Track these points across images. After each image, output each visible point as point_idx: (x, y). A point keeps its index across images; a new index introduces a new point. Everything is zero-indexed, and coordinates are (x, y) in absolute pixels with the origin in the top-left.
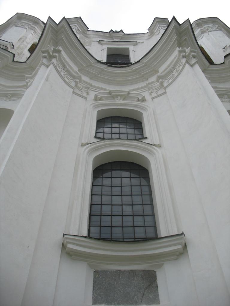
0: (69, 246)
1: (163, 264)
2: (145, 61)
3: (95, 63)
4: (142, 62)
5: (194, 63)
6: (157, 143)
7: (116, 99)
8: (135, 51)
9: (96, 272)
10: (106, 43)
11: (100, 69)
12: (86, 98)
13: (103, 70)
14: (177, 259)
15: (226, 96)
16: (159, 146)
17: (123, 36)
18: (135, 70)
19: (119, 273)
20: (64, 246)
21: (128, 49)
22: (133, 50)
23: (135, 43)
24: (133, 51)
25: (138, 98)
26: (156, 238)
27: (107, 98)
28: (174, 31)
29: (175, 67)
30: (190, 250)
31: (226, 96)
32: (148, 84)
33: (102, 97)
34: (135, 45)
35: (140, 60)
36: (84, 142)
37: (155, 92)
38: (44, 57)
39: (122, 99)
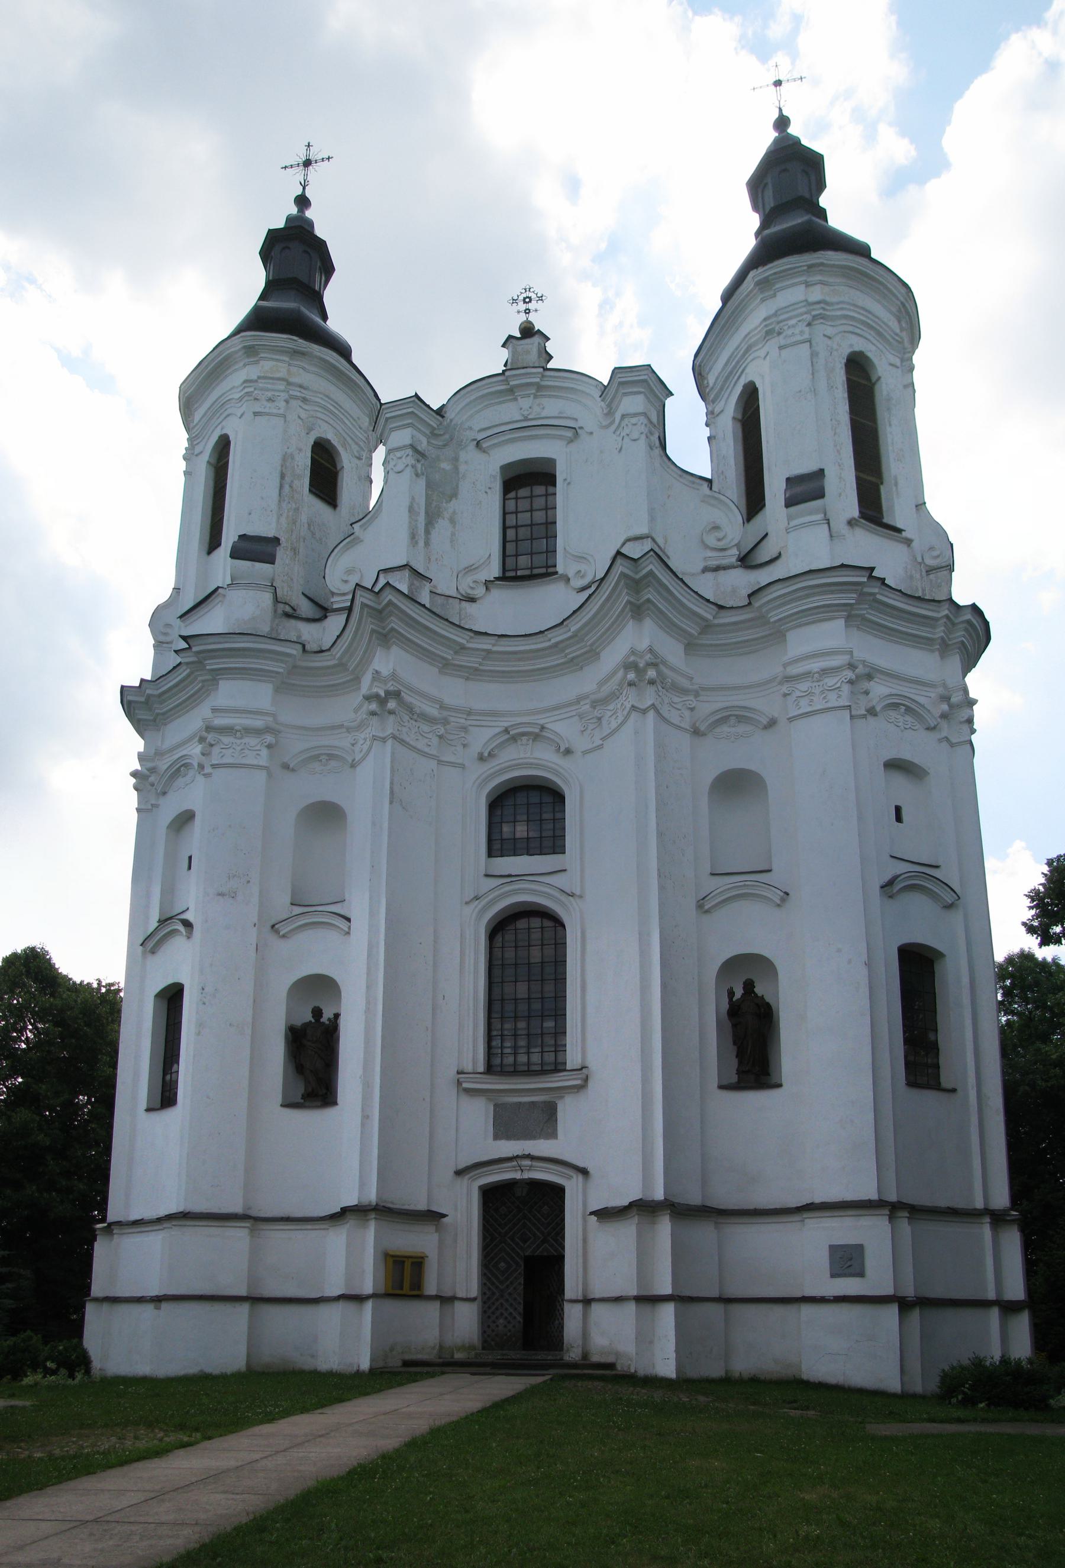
0: (465, 1085)
1: (563, 1097)
2: (574, 626)
3: (471, 638)
4: (567, 626)
5: (648, 708)
6: (578, 893)
7: (519, 740)
8: (569, 484)
9: (496, 1106)
10: (496, 441)
11: (483, 650)
12: (463, 766)
13: (489, 652)
14: (578, 1092)
15: (733, 720)
16: (581, 897)
17: (543, 376)
18: (556, 645)
19: (520, 1104)
20: (459, 1083)
22: (565, 480)
23: (569, 434)
24: (568, 481)
25: (558, 744)
26: (558, 1067)
27: (501, 746)
28: (622, 583)
29: (621, 688)
30: (590, 1084)
31: (733, 720)
32: (579, 700)
33: (492, 750)
34: (571, 441)
35: (564, 620)
36: (467, 900)
37: (589, 731)
38: (373, 713)
39: (531, 741)
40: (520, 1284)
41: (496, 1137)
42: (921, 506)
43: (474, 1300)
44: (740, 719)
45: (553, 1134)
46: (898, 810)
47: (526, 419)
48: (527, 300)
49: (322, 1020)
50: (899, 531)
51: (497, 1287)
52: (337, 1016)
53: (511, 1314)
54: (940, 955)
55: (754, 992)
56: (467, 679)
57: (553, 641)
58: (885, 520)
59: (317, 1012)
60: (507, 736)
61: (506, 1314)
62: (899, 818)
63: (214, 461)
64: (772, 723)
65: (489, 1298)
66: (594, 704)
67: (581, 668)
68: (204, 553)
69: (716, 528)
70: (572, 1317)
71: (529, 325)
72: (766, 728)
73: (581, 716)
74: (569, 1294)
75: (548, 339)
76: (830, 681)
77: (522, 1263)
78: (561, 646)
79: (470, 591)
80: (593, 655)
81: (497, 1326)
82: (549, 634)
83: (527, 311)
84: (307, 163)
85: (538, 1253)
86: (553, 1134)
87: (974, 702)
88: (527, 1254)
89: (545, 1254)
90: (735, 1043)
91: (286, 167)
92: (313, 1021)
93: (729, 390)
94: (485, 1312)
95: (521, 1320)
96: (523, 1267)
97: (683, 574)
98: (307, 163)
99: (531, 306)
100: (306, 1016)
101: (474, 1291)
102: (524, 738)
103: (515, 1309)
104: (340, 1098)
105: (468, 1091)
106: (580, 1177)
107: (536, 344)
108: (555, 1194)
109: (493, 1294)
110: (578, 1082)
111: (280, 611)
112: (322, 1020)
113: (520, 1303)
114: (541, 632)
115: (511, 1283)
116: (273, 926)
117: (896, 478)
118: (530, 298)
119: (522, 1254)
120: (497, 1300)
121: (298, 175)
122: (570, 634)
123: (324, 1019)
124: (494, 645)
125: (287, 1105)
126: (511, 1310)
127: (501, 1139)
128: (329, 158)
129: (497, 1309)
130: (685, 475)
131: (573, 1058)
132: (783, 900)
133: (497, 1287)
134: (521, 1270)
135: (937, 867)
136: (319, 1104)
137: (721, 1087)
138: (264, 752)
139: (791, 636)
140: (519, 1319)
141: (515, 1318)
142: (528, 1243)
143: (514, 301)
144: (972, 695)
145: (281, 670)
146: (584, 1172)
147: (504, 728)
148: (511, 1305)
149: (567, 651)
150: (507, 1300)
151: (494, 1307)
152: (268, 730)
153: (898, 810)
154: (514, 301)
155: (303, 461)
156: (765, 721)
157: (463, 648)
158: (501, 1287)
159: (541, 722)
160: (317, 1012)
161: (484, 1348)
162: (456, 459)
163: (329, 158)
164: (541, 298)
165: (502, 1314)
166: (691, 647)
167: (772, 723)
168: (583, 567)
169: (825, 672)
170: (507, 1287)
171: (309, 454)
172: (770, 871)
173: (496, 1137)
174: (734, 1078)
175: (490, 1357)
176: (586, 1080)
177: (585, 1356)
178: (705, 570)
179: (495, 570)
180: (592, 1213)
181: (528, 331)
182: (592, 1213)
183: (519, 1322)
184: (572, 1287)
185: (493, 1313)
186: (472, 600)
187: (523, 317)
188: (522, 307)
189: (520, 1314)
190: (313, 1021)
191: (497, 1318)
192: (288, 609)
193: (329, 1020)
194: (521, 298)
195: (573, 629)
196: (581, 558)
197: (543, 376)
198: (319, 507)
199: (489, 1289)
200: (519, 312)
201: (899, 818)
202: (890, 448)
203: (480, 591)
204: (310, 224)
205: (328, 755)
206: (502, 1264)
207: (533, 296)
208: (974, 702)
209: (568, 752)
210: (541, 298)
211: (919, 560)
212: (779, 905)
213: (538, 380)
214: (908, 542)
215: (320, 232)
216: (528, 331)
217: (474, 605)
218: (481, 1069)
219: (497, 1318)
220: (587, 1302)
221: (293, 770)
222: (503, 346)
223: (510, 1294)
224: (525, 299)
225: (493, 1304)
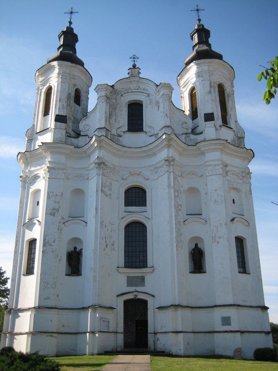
0: (120, 271)
2: (150, 147)
6: (150, 217)
8: (146, 108)
13: (126, 151)
18: (144, 151)
21: (142, 101)
30: (155, 271)
32: (150, 166)
41: (128, 286)
42: (236, 121)
43: (122, 333)
44: (193, 174)
45: (144, 286)
46: (233, 200)
47: (135, 89)
48: (134, 58)
49: (76, 250)
50: (232, 129)
52: (81, 249)
54: (245, 239)
55: (198, 247)
56: (120, 158)
57: (144, 150)
58: (228, 126)
59: (75, 248)
60: (130, 174)
62: (234, 203)
63: (46, 91)
64: (202, 176)
66: (156, 168)
67: (151, 157)
68: (43, 116)
69: (186, 123)
70: (151, 338)
71: (135, 65)
72: (200, 177)
73: (151, 170)
74: (149, 331)
75: (140, 69)
76: (217, 167)
78: (146, 151)
79: (120, 134)
80: (155, 154)
82: (143, 148)
83: (134, 61)
84: (71, 13)
85: (139, 319)
86: (144, 286)
87: (251, 173)
88: (137, 319)
89: (142, 320)
90: (193, 261)
91: (65, 13)
92: (74, 250)
93: (187, 87)
94: (124, 337)
97: (178, 135)
98: (71, 13)
99: (135, 60)
100: (73, 249)
101: (122, 331)
102: (135, 175)
104: (83, 273)
105: (120, 273)
106: (152, 297)
107: (137, 70)
108: (145, 302)
109: (127, 331)
110: (151, 271)
111: (67, 135)
112: (76, 250)
113: (134, 334)
114: (141, 147)
116: (64, 223)
117: (230, 115)
118: (135, 58)
119: (135, 320)
121: (69, 16)
122: (148, 149)
123: (77, 250)
124: (127, 150)
125: (67, 275)
127: (129, 286)
128: (78, 12)
129: (128, 336)
130: (177, 109)
131: (149, 263)
132: (205, 223)
134: (135, 324)
135: (244, 215)
136: (76, 275)
137: (190, 273)
138: (63, 175)
139: (206, 154)
140: (135, 339)
142: (137, 317)
143: (131, 58)
144: (250, 171)
145: (68, 153)
146: (153, 296)
147: (129, 172)
148: (132, 335)
149: (147, 153)
151: (127, 335)
152: (64, 169)
153: (233, 200)
154: (131, 58)
155: (73, 94)
156: (200, 175)
157: (119, 150)
159: (140, 171)
160: (75, 248)
161: (124, 348)
162: (116, 99)
163: (78, 12)
164: (138, 58)
166: (181, 154)
167: (202, 176)
168: (150, 130)
169: (216, 165)
171: (74, 93)
172: (201, 215)
173: (128, 286)
174: (193, 270)
175: (127, 350)
177: (155, 349)
178: (182, 134)
179: (127, 130)
180: (156, 308)
181: (134, 66)
182: (156, 308)
184: (150, 329)
186: (120, 136)
187: (133, 63)
188: (133, 60)
190: (74, 250)
191: (128, 338)
192: (69, 135)
193: (79, 250)
194: (133, 57)
195: (150, 148)
196: (150, 127)
197: (139, 79)
198: (77, 106)
200: (132, 61)
201: (234, 203)
202: (229, 107)
203: (122, 134)
204: (72, 29)
205: (80, 176)
206: (129, 323)
207: (136, 57)
208: (251, 173)
209: (147, 179)
210: (138, 58)
211: (237, 135)
212: (204, 224)
213: (138, 80)
214: (234, 131)
215: (75, 32)
216: (134, 66)
217: (121, 138)
218: (124, 267)
219: (128, 338)
220: (155, 333)
221: (70, 179)
222: (128, 70)
224: (133, 58)
225: (127, 334)
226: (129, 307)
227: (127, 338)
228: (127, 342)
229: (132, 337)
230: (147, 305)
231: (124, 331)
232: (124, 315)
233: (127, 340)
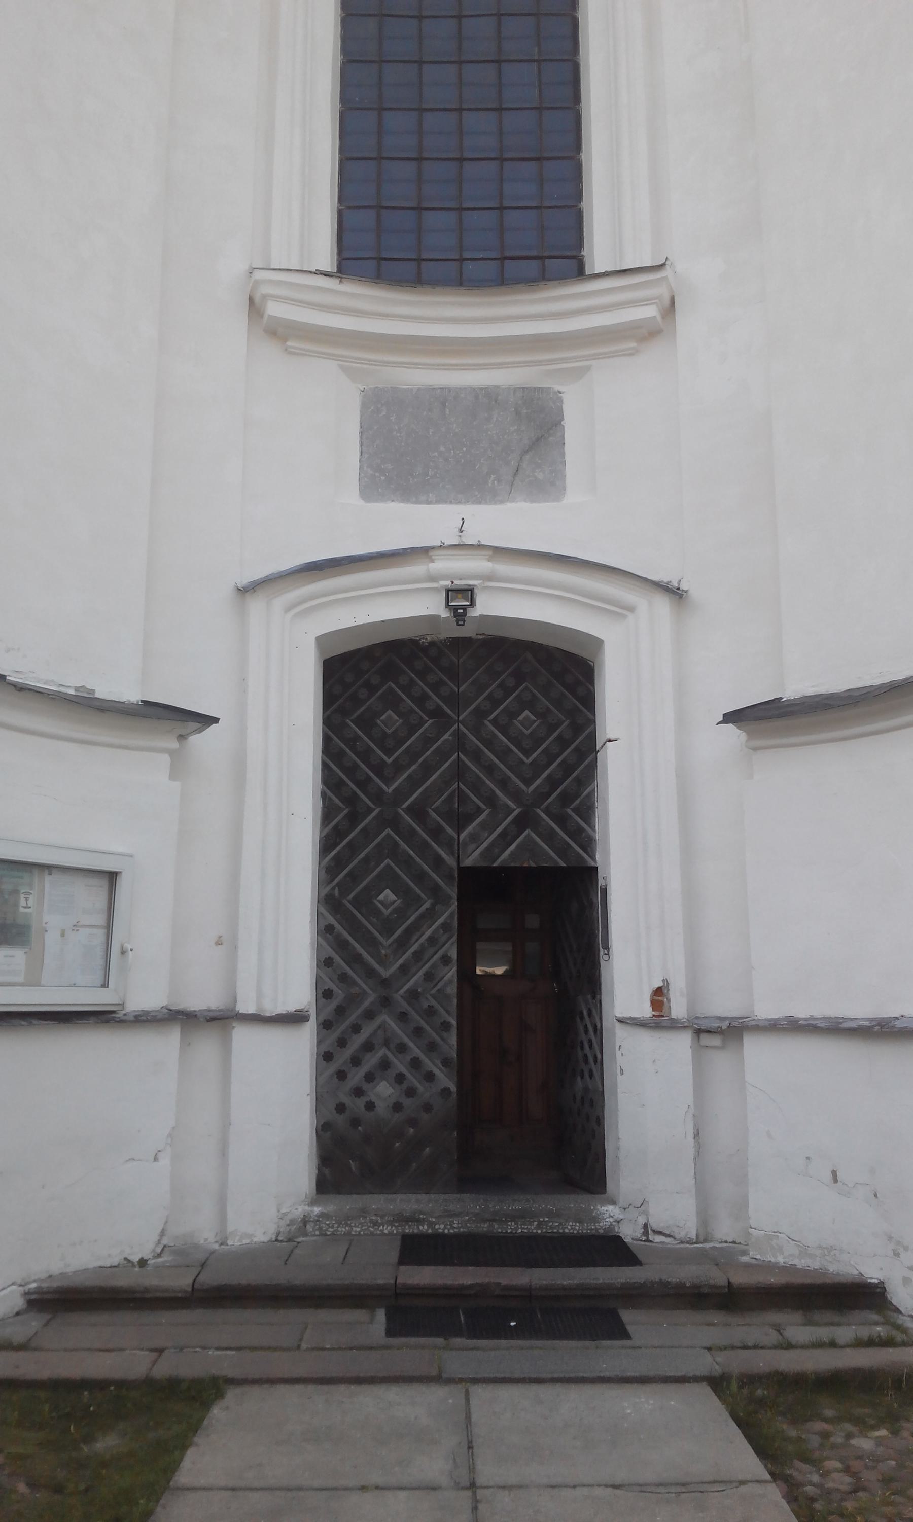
0: (274, 309)
1: (588, 368)
14: (633, 353)
20: (254, 307)
40: (446, 960)
43: (295, 1019)
51: (370, 973)
53: (415, 1064)
61: (399, 1065)
65: (340, 1011)
77: (453, 892)
81: (370, 1106)
85: (504, 858)
88: (468, 862)
94: (326, 1057)
95: (454, 1088)
96: (454, 906)
103: (432, 1047)
106: (662, 605)
110: (650, 312)
113: (446, 1026)
115: (418, 956)
119: (450, 861)
120: (369, 1015)
126: (416, 1051)
129: (368, 1047)
133: (370, 973)
134: (450, 912)
140: (446, 1080)
141: (430, 1077)
142: (470, 829)
148: (418, 1032)
150: (403, 1017)
151: (357, 1041)
158: (385, 973)
165: (385, 1065)
170: (404, 970)
176: (670, 308)
183: (446, 1091)
185: (356, 1061)
189: (446, 1062)
191: (370, 1077)
199: (343, 978)
206: (388, 895)
219: (370, 1077)
223: (413, 996)
226: (390, 720)
227: (356, 1077)
228: (355, 1122)
229: (415, 1064)
230: (588, 701)
231: (324, 994)
232: (328, 814)
233: (358, 1092)
